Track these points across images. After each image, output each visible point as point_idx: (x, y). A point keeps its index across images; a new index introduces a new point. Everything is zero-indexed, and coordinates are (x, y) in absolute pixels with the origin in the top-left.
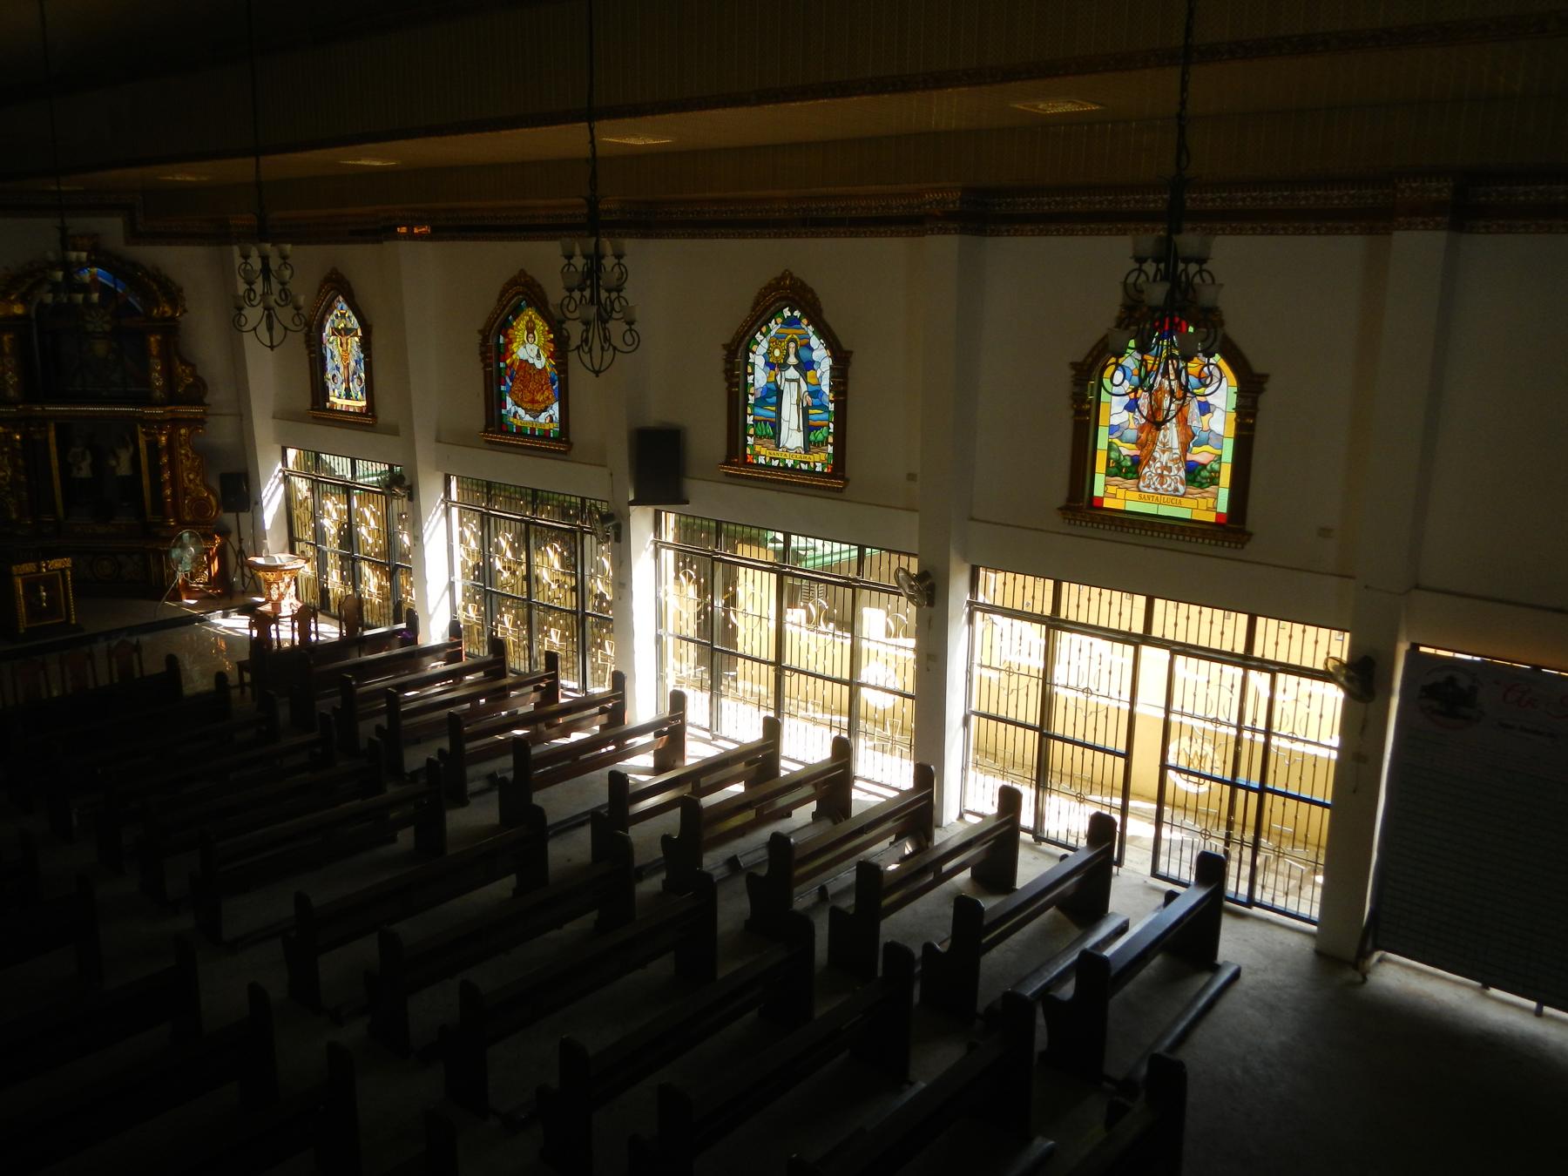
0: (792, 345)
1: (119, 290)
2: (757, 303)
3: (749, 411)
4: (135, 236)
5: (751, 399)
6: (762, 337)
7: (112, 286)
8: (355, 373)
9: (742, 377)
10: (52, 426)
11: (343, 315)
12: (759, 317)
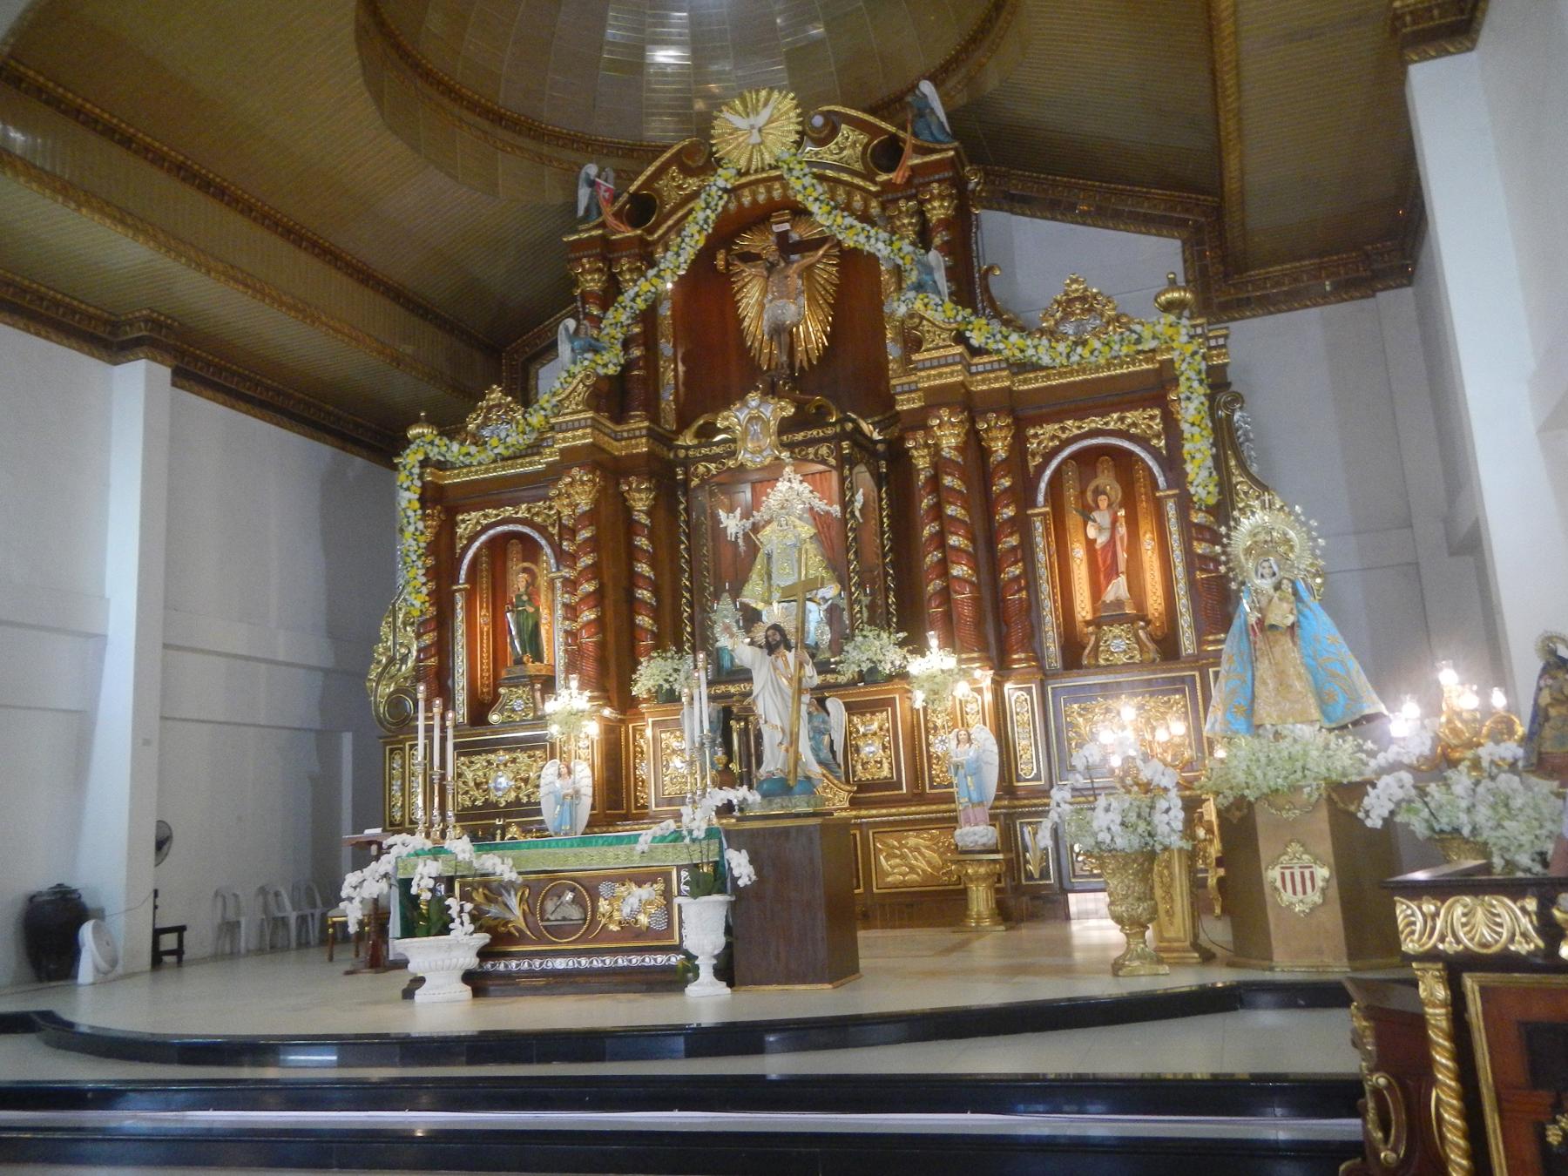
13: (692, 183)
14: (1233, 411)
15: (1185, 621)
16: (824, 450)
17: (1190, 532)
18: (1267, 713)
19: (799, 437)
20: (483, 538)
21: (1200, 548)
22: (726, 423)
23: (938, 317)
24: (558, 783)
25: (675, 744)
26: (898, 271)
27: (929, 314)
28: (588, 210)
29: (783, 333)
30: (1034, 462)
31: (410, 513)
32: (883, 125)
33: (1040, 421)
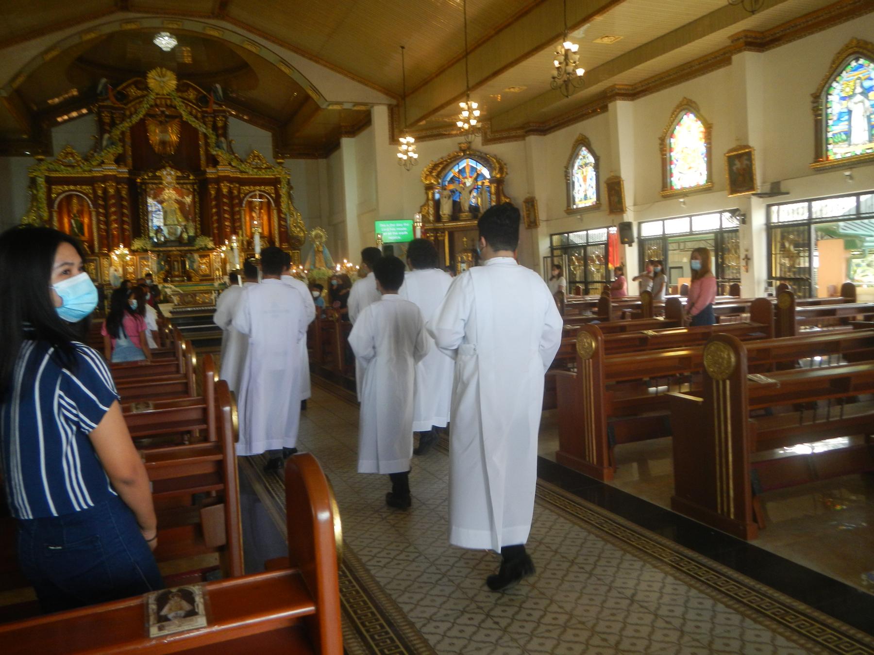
0: (858, 81)
1: (478, 168)
2: (834, 62)
3: (829, 129)
4: (487, 141)
5: (830, 122)
6: (837, 84)
7: (475, 166)
8: (590, 185)
9: (824, 110)
10: (447, 233)
11: (584, 157)
12: (835, 70)
13: (139, 93)
14: (290, 190)
15: (277, 240)
16: (189, 186)
17: (280, 219)
18: (317, 265)
19: (182, 181)
20: (64, 195)
21: (283, 223)
22: (160, 174)
23: (225, 157)
24: (116, 273)
25: (145, 263)
26: (206, 137)
27: (222, 156)
28: (101, 92)
29: (163, 143)
30: (242, 195)
31: (42, 185)
32: (202, 91)
33: (244, 185)
